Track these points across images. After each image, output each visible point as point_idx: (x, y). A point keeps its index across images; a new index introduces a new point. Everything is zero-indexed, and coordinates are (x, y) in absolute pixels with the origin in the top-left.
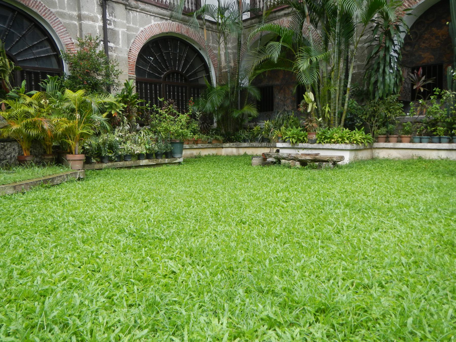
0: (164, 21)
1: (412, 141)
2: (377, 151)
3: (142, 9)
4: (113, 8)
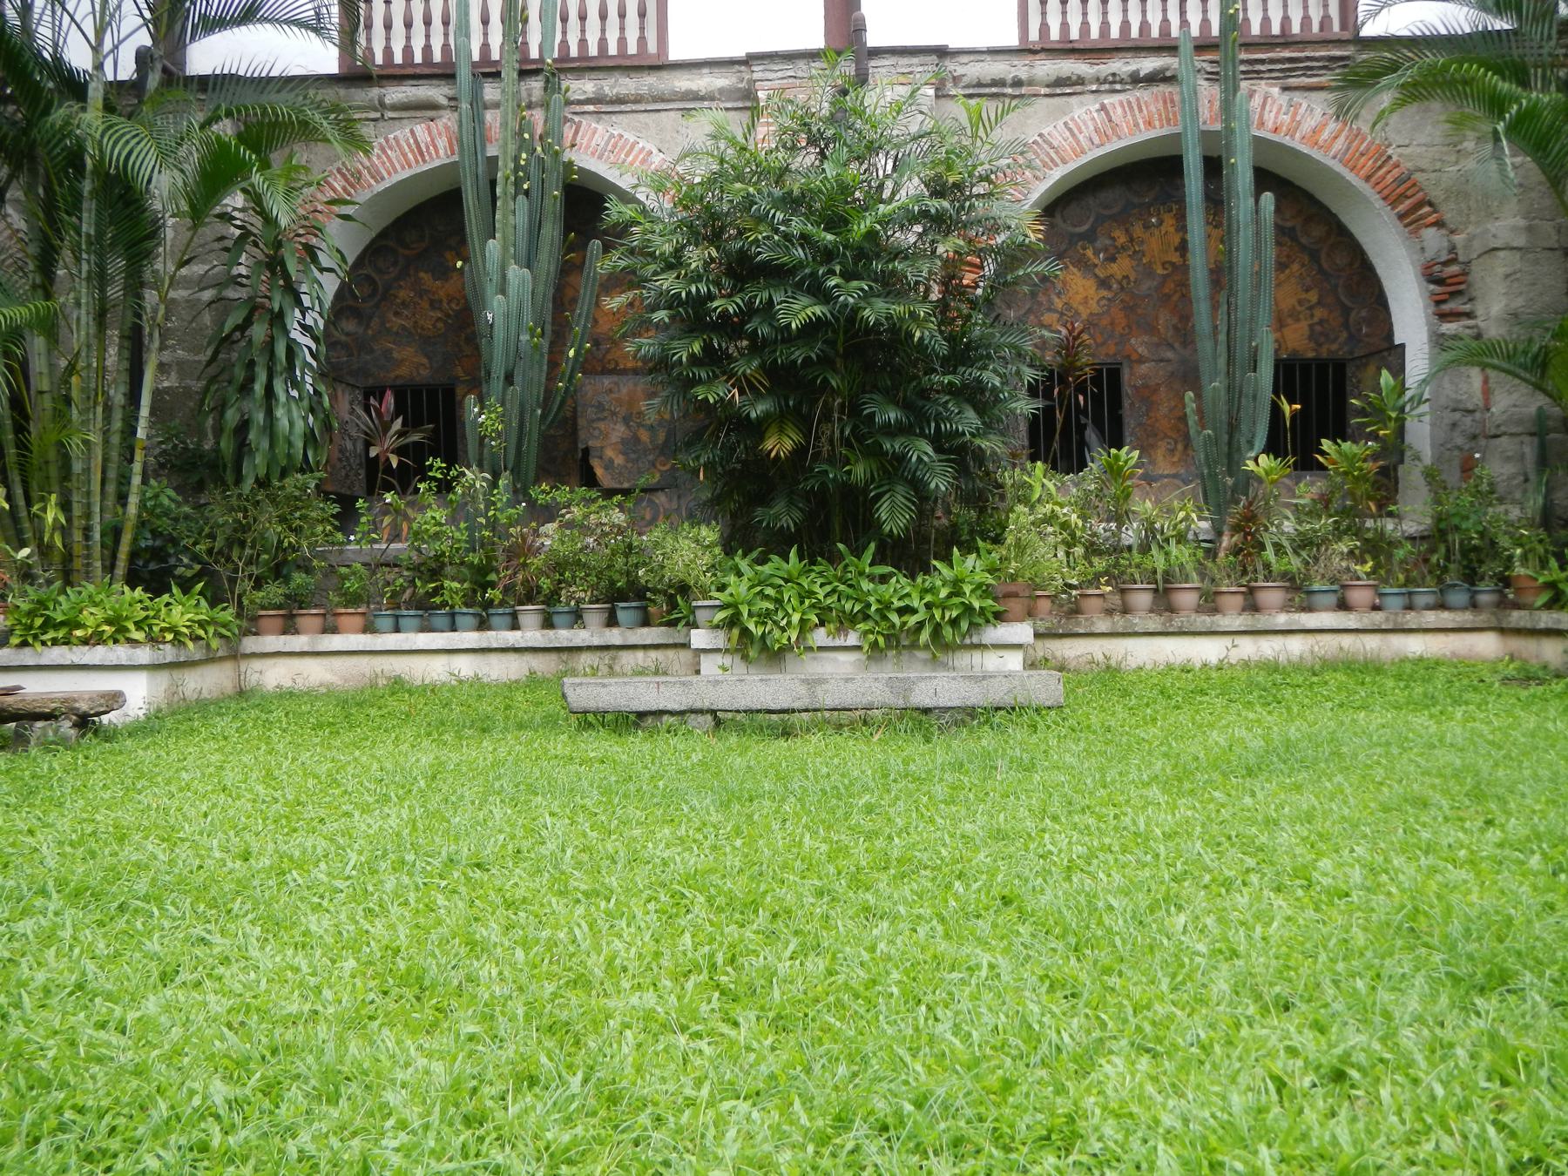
1: (369, 629)
2: (257, 665)
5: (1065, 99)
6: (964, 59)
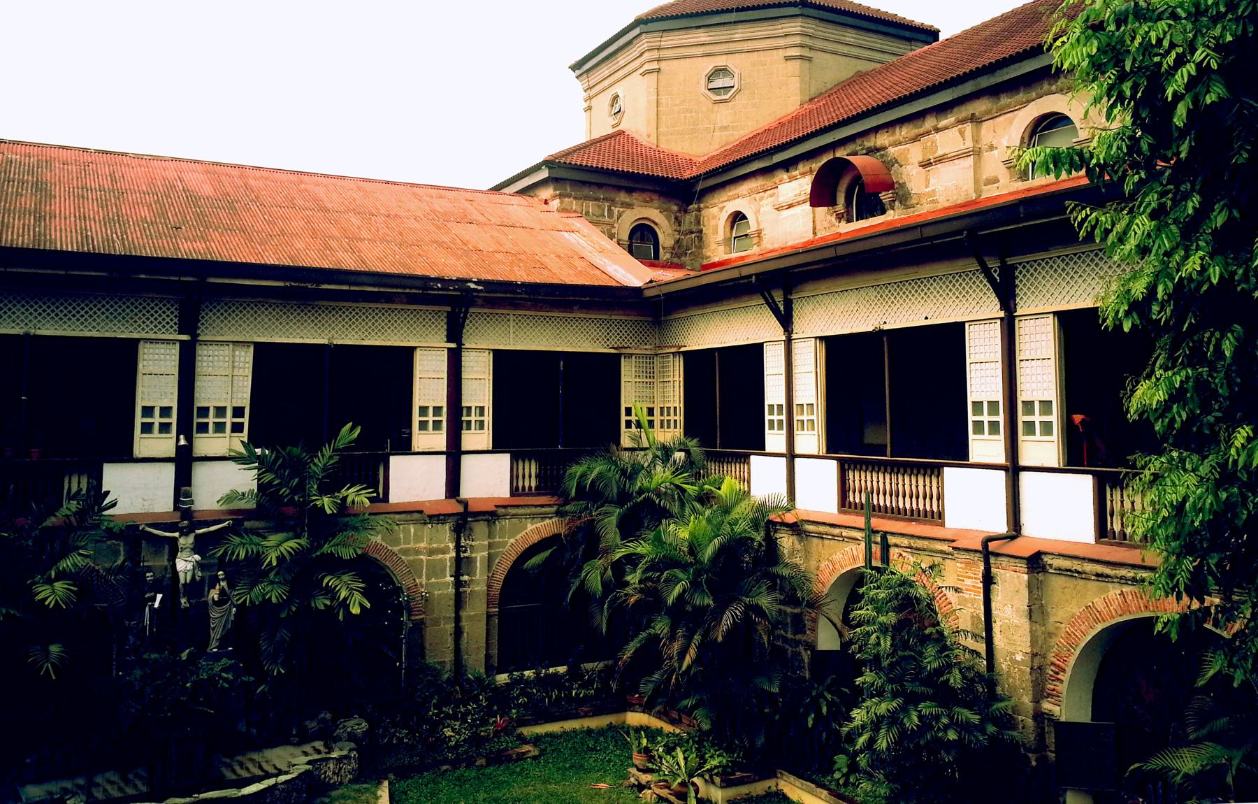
0: (547, 521)
3: (513, 515)
4: (471, 529)
5: (1105, 583)
6: (1051, 557)
